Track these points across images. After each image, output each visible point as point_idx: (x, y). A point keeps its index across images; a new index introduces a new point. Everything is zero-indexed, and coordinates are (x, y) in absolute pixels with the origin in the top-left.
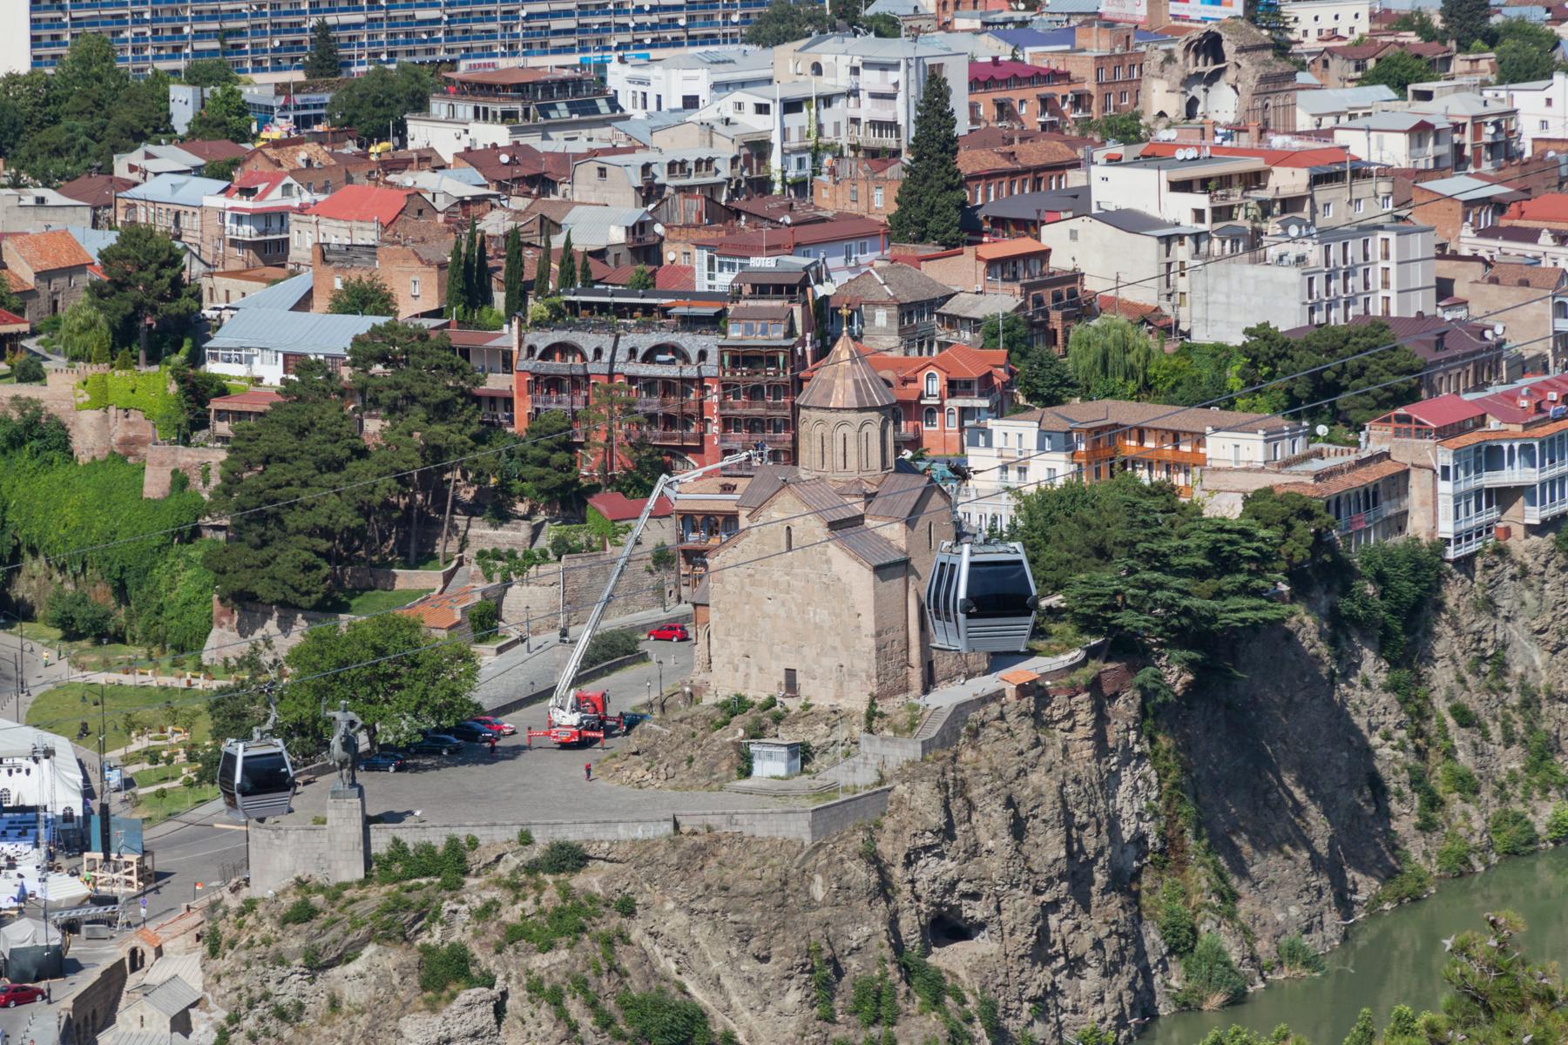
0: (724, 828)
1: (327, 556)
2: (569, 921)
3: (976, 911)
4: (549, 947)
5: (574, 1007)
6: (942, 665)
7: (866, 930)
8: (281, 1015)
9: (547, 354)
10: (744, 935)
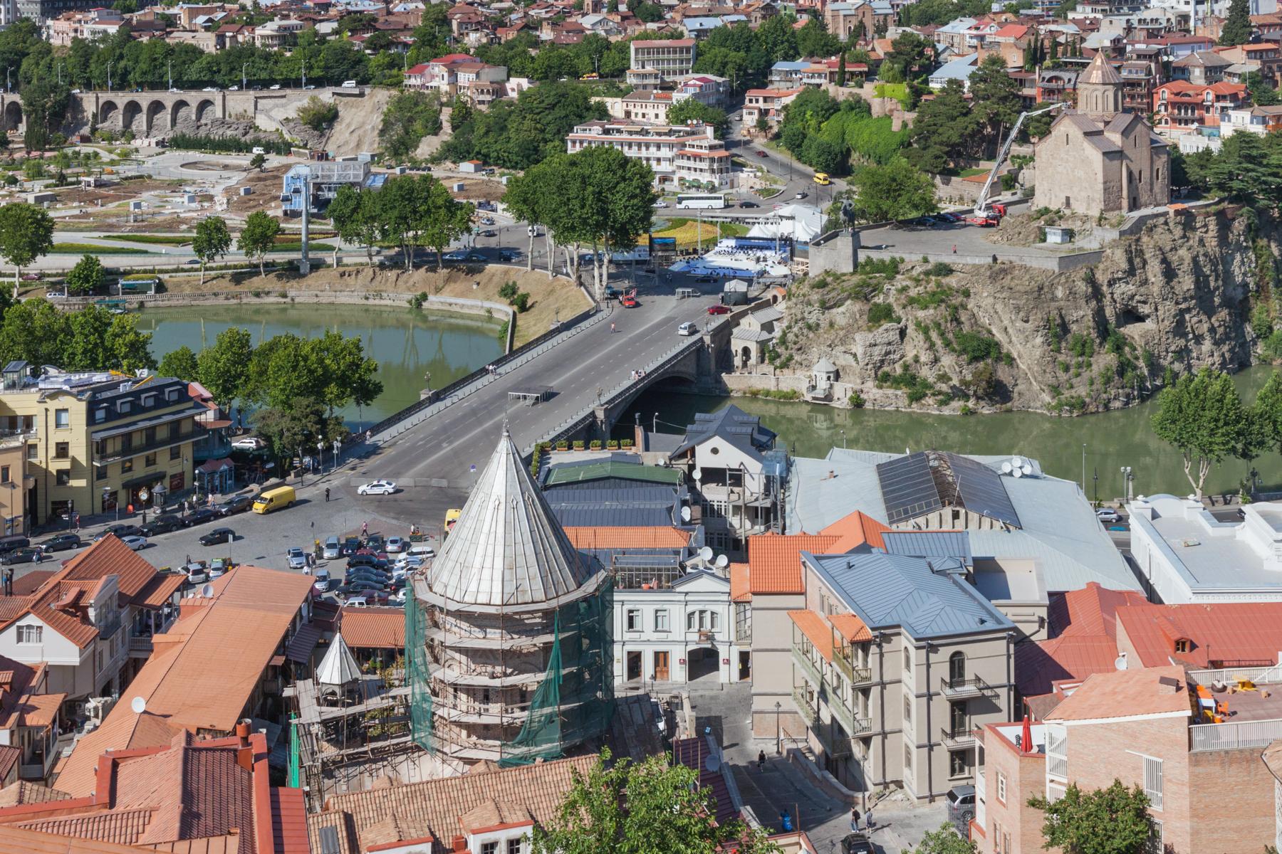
0: (1017, 262)
1: (946, 153)
2: (938, 298)
3: (1144, 309)
4: (926, 307)
5: (934, 335)
6: (1144, 198)
7: (1082, 313)
8: (810, 327)
10: (1018, 309)
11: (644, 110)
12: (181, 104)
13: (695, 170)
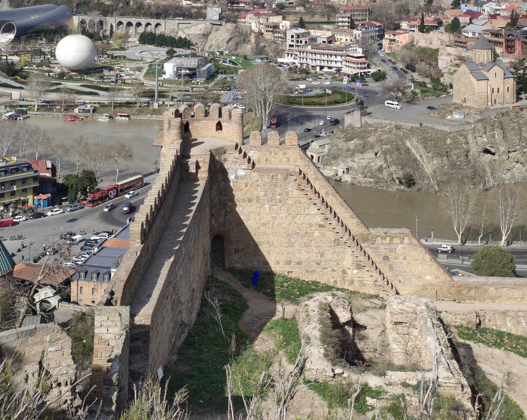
9: (509, 35)
11: (341, 37)
12: (148, 24)
13: (349, 67)
